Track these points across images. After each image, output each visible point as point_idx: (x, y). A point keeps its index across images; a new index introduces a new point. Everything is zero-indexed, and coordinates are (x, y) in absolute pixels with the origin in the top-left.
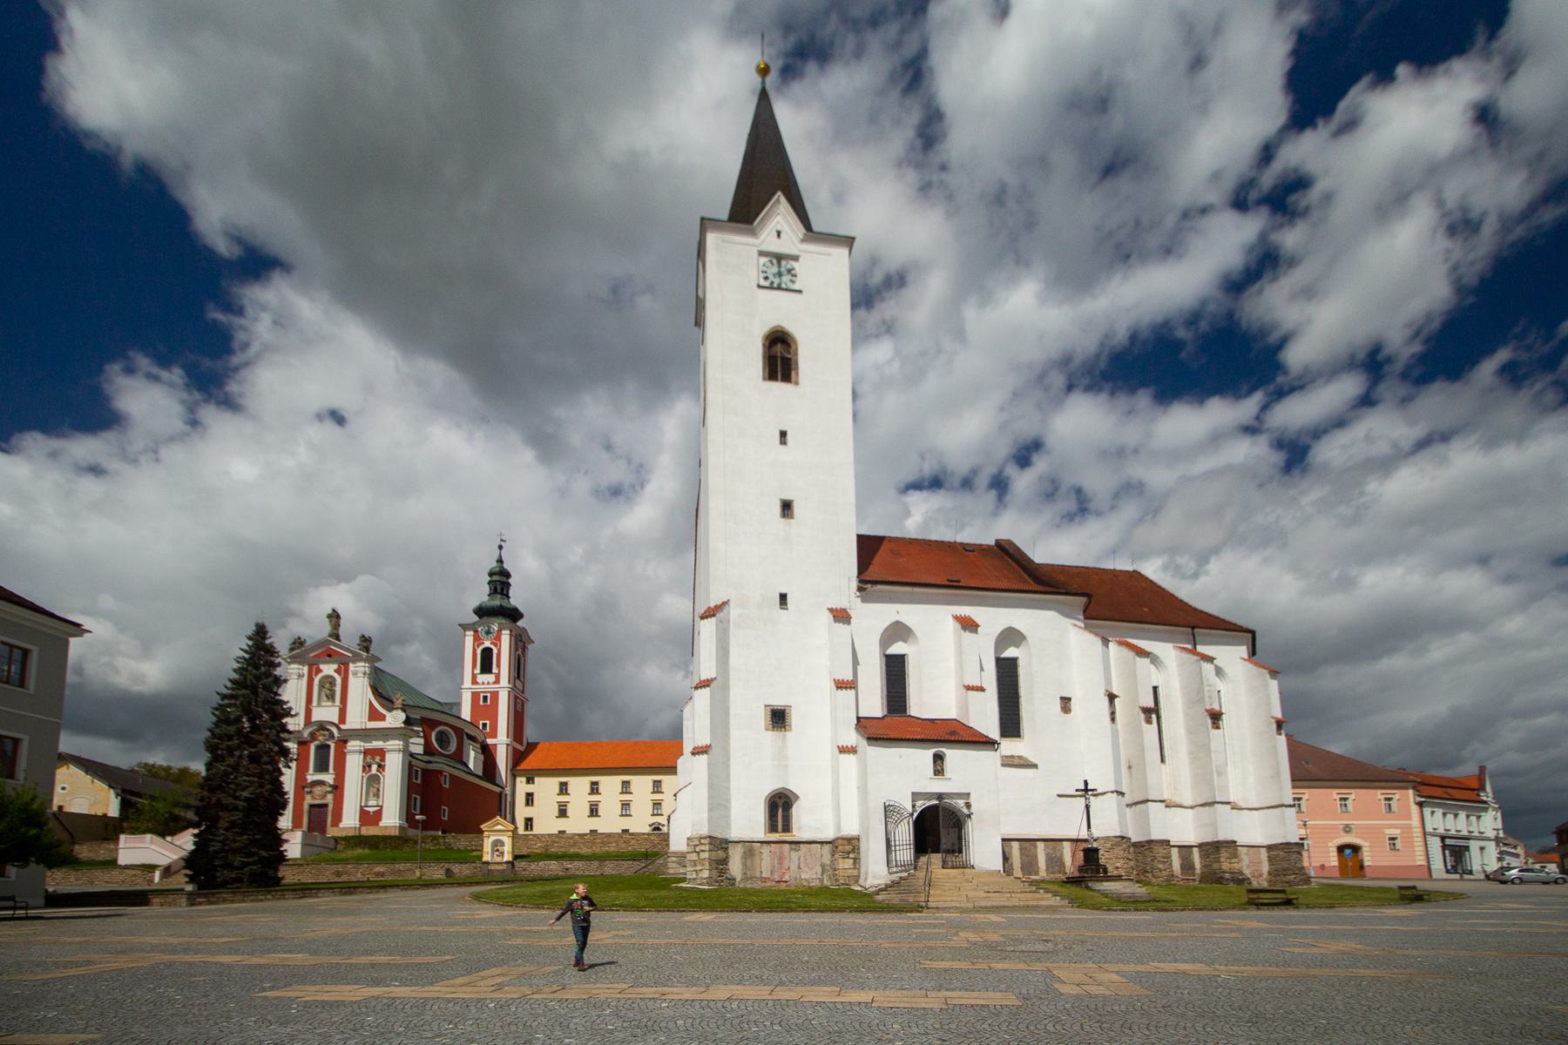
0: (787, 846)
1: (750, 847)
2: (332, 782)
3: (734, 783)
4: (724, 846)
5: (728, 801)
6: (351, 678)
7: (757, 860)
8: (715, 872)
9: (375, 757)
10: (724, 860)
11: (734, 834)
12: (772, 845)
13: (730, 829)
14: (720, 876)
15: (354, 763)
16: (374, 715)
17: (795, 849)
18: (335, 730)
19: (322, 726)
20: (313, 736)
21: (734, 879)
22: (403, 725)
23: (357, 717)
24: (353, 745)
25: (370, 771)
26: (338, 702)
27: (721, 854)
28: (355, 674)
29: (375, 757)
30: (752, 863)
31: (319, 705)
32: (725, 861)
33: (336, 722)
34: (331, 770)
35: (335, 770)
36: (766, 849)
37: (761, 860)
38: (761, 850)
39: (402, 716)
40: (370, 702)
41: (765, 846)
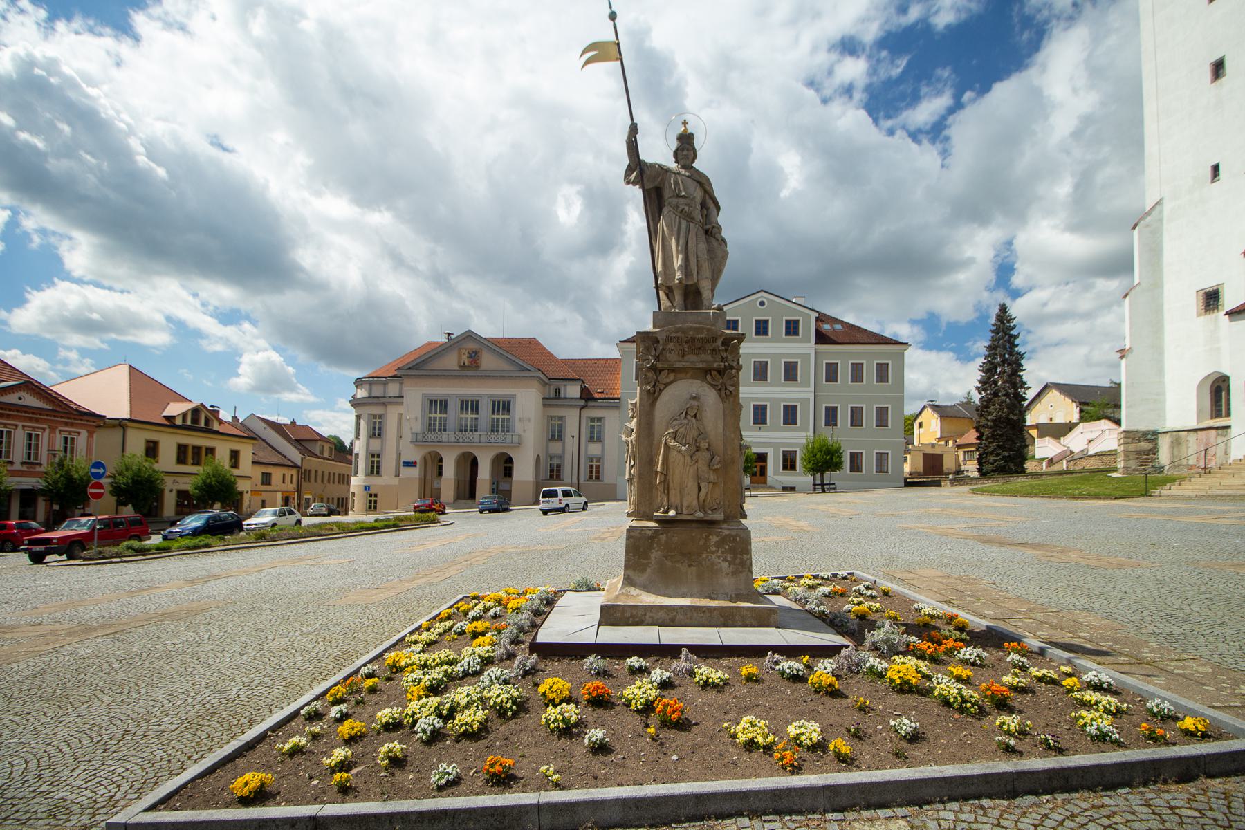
0: (1214, 432)
1: (1177, 436)
3: (1168, 378)
4: (1149, 437)
5: (1162, 393)
7: (1183, 448)
8: (1133, 464)
10: (1150, 450)
11: (1172, 422)
12: (1199, 432)
13: (1165, 420)
14: (1141, 465)
17: (1222, 435)
21: (1163, 467)
27: (1145, 445)
30: (1179, 451)
32: (1154, 451)
36: (1192, 437)
37: (1188, 448)
38: (1188, 438)
41: (1191, 433)
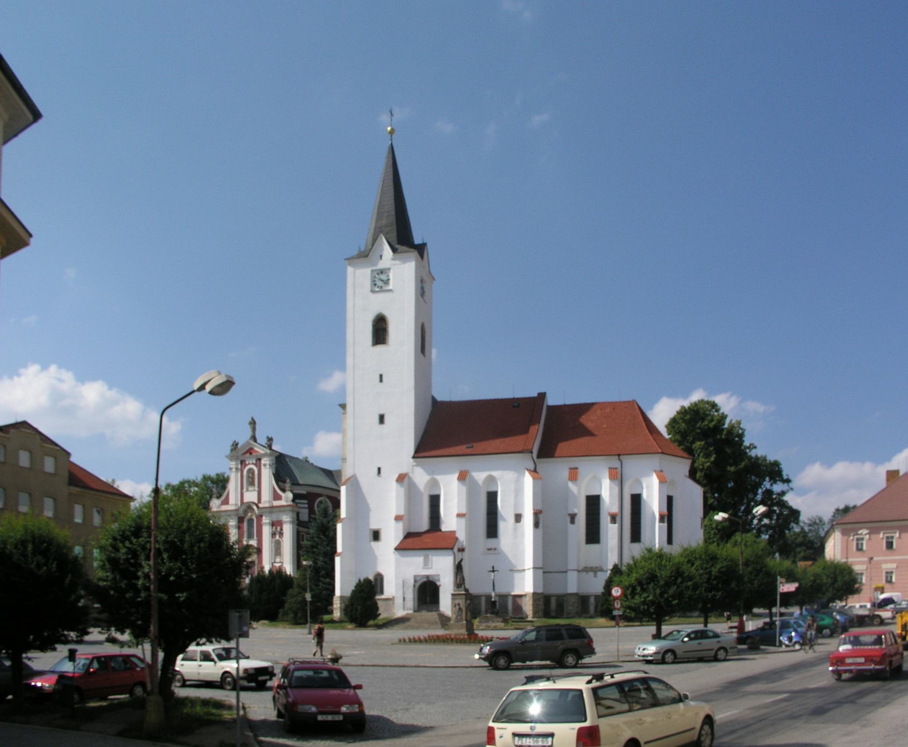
2: (256, 545)
6: (263, 467)
9: (276, 525)
15: (266, 531)
16: (277, 497)
18: (255, 507)
19: (249, 507)
20: (246, 512)
22: (292, 503)
23: (266, 496)
24: (265, 520)
25: (275, 537)
26: (256, 488)
28: (265, 465)
29: (276, 525)
31: (247, 490)
33: (256, 501)
34: (255, 537)
35: (257, 536)
39: (290, 495)
40: (274, 488)
